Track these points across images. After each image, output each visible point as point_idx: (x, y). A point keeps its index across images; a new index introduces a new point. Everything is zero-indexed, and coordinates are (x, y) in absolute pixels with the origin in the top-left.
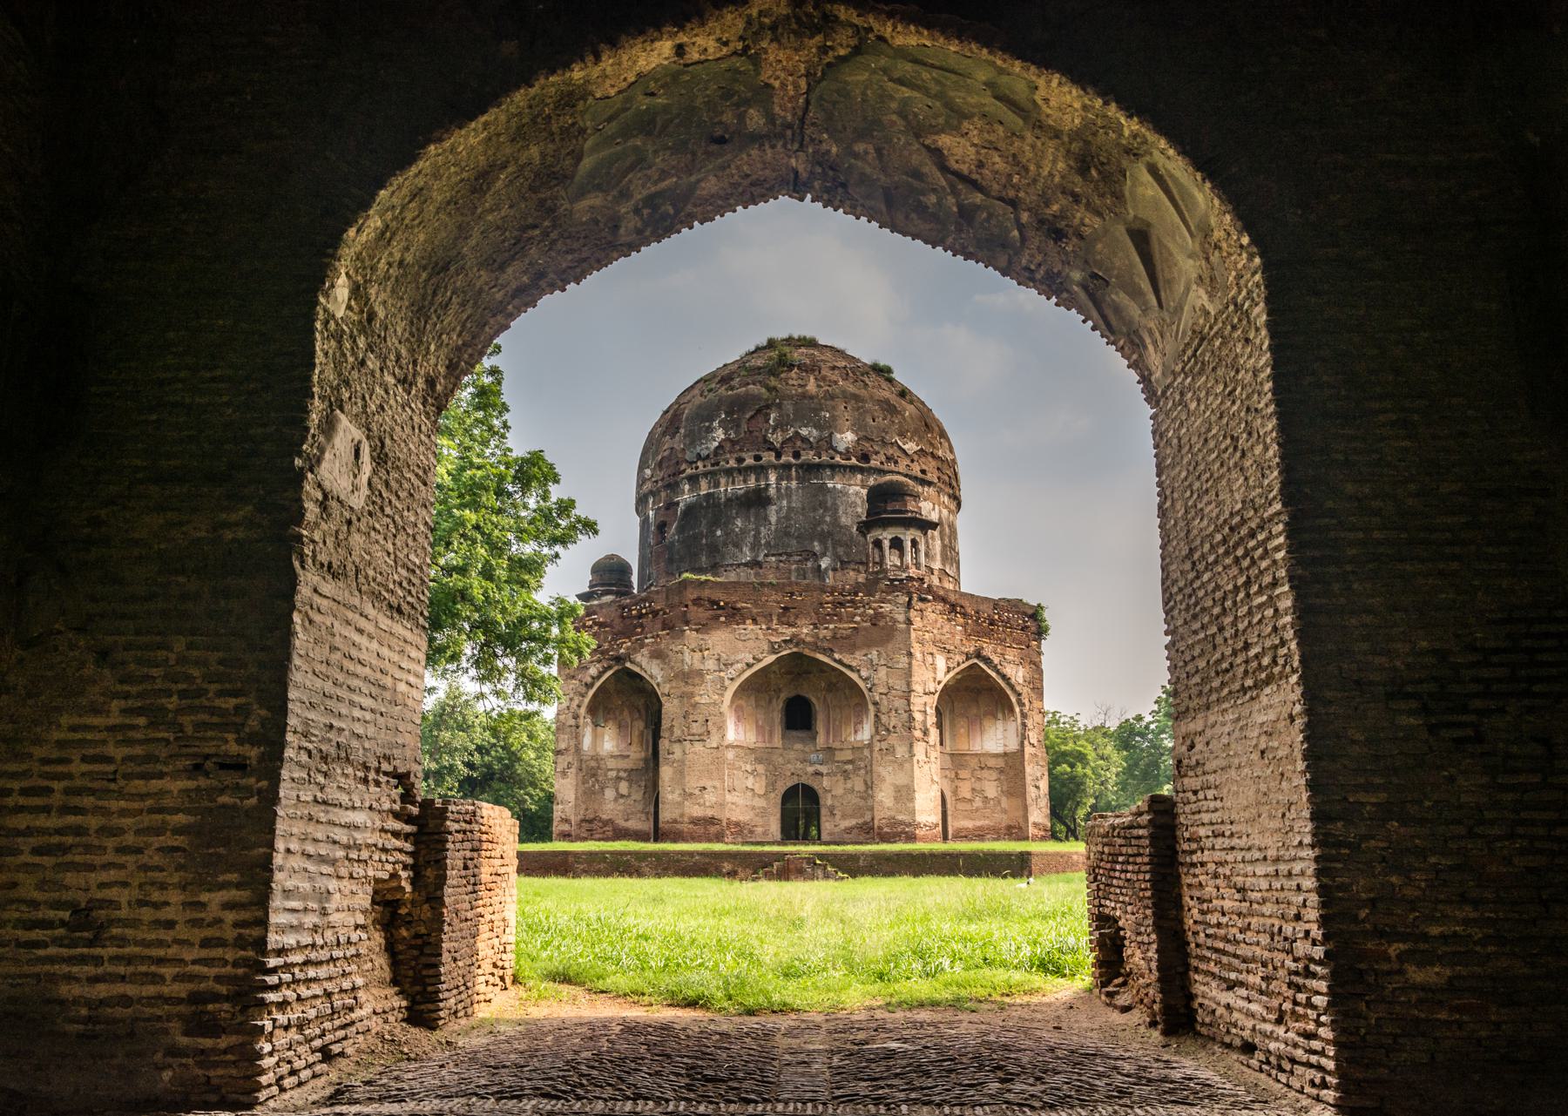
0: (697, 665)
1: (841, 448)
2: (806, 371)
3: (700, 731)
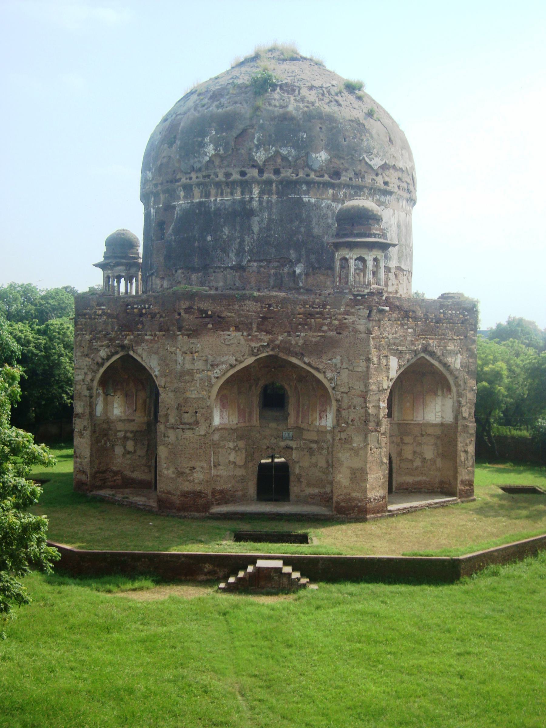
0: (188, 366)
1: (316, 166)
2: (288, 93)
3: (191, 420)
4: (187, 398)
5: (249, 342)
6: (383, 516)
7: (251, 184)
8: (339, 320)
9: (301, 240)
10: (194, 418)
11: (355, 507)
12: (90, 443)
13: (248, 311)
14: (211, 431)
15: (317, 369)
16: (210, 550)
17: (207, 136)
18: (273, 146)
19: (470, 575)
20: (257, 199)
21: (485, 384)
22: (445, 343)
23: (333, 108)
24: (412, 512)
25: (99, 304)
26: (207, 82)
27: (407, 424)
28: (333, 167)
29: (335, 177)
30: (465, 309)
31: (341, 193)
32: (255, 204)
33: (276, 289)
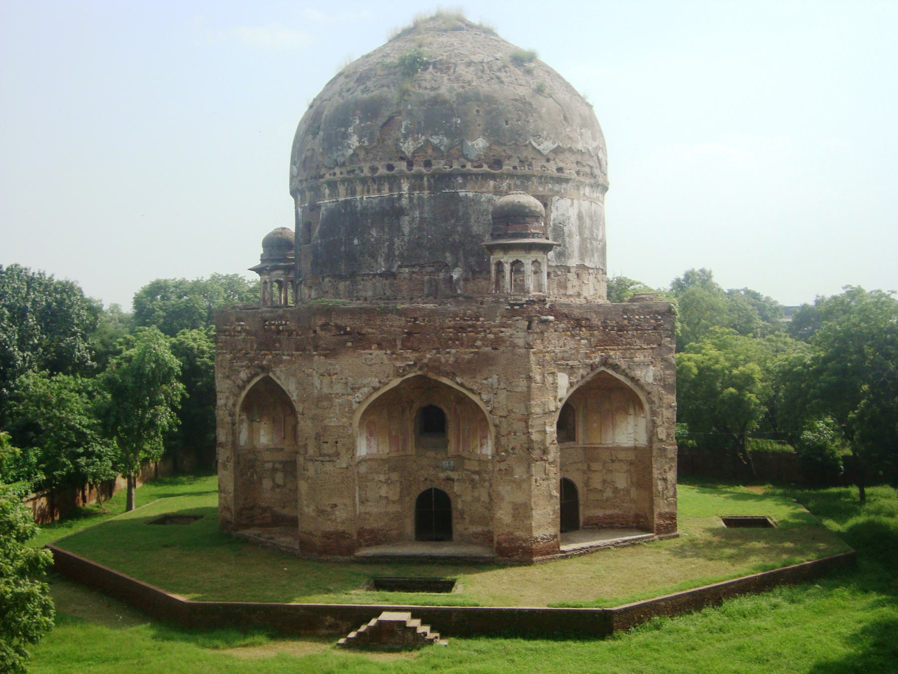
0: (326, 390)
1: (473, 156)
2: (441, 71)
3: (331, 451)
6: (554, 559)
7: (400, 181)
8: (495, 334)
9: (457, 241)
10: (334, 449)
11: (519, 547)
12: (233, 476)
13: (391, 326)
14: (353, 463)
15: (472, 391)
16: (333, 601)
17: (350, 126)
18: (422, 135)
19: (626, 629)
20: (407, 196)
21: (732, 390)
23: (493, 86)
24: (592, 552)
25: (239, 319)
26: (358, 60)
27: (595, 448)
28: (494, 156)
29: (496, 166)
31: (505, 184)
32: (404, 202)
33: (431, 298)
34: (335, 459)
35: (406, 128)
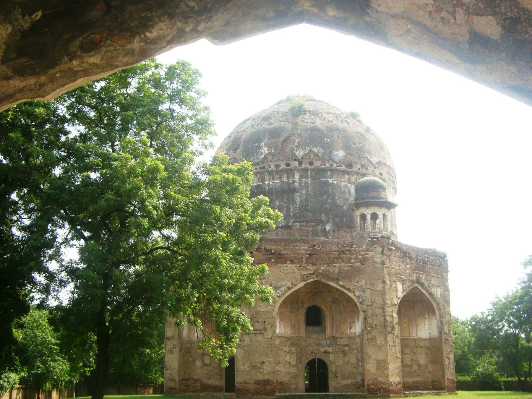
1: (337, 160)
2: (315, 115)
3: (261, 328)
4: (258, 311)
5: (301, 271)
8: (362, 255)
13: (299, 250)
15: (349, 290)
18: (308, 146)
22: (430, 278)
24: (419, 396)
27: (406, 339)
28: (348, 161)
30: (440, 257)
31: (353, 178)
32: (297, 184)
34: (264, 332)
35: (298, 143)
